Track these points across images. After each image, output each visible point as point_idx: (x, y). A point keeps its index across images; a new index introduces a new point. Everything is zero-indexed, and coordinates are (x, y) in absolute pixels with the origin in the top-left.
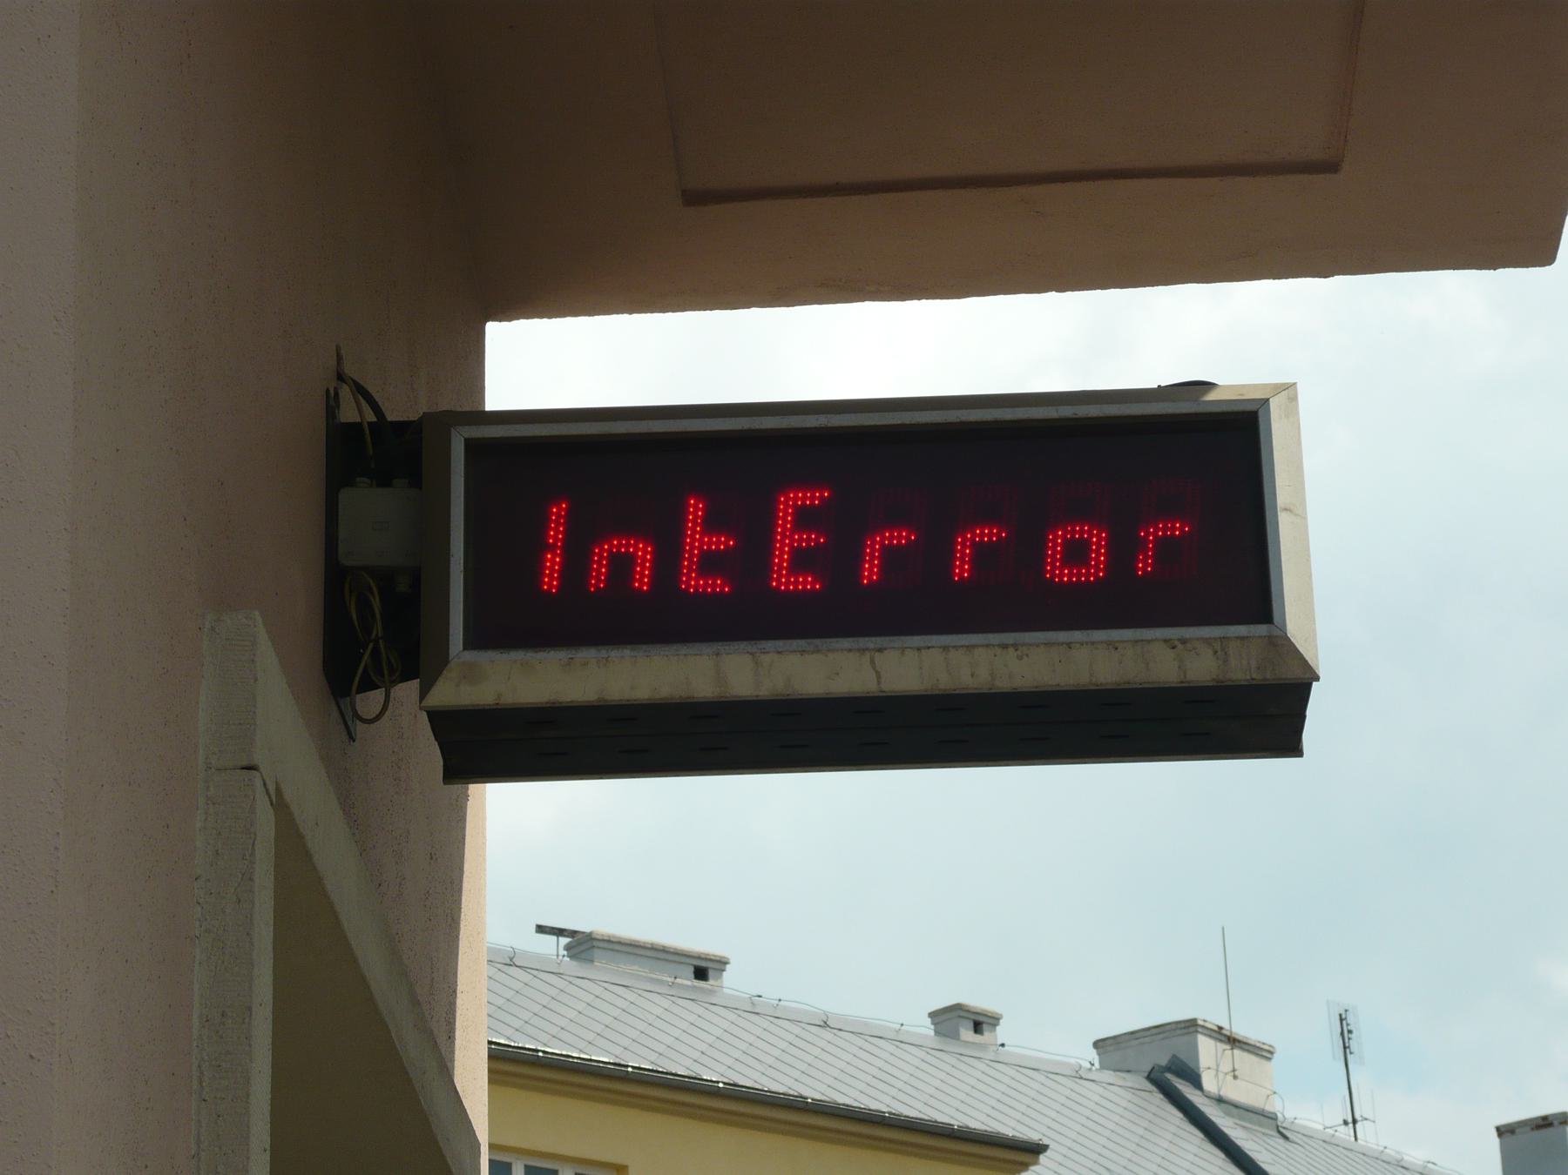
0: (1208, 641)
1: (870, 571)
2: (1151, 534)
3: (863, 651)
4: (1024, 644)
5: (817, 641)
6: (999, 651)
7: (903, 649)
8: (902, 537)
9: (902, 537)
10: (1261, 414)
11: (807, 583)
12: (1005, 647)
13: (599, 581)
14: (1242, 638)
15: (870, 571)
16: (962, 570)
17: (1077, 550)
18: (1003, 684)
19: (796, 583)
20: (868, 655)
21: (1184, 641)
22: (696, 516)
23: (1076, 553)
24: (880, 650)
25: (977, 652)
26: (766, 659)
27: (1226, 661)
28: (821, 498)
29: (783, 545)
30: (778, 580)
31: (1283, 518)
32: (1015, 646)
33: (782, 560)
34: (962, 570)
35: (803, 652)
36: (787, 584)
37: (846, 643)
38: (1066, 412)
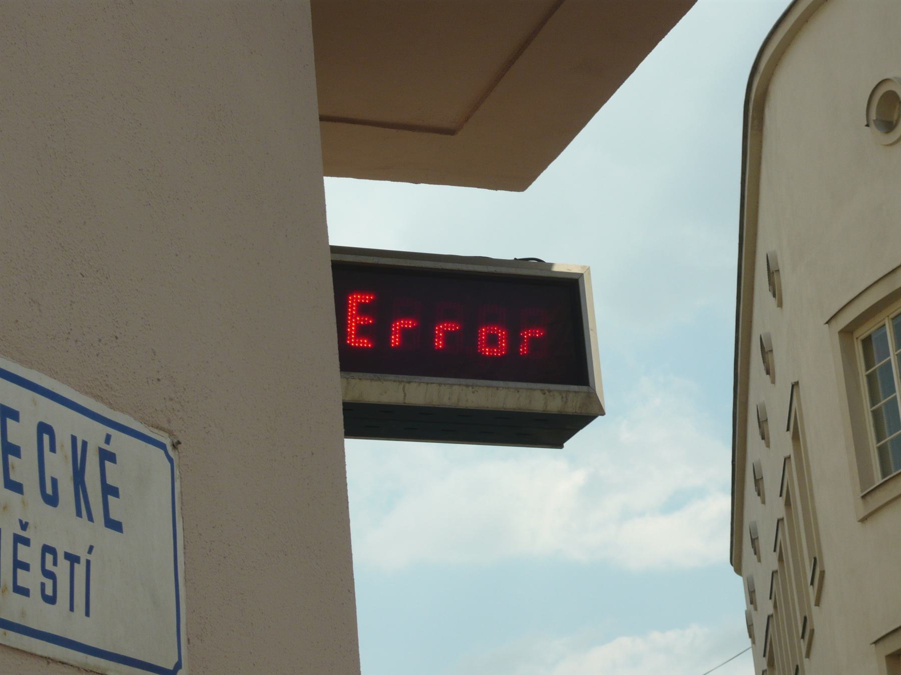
0: (560, 392)
1: (395, 341)
2: (398, 325)
3: (401, 382)
4: (477, 386)
5: (378, 375)
6: (465, 388)
7: (420, 383)
8: (410, 324)
9: (410, 324)
10: (580, 281)
11: (365, 343)
12: (467, 386)
13: (395, 341)
14: (575, 392)
15: (395, 341)
16: (439, 344)
17: (492, 341)
18: (463, 404)
19: (359, 343)
20: (402, 386)
21: (549, 391)
22: (352, 308)
23: (492, 341)
24: (409, 382)
25: (454, 387)
26: (353, 381)
27: (566, 402)
28: (369, 299)
29: (352, 322)
30: (350, 340)
31: (591, 333)
32: (472, 386)
33: (352, 330)
34: (439, 344)
35: (372, 380)
36: (355, 343)
37: (392, 377)
38: (491, 269)
